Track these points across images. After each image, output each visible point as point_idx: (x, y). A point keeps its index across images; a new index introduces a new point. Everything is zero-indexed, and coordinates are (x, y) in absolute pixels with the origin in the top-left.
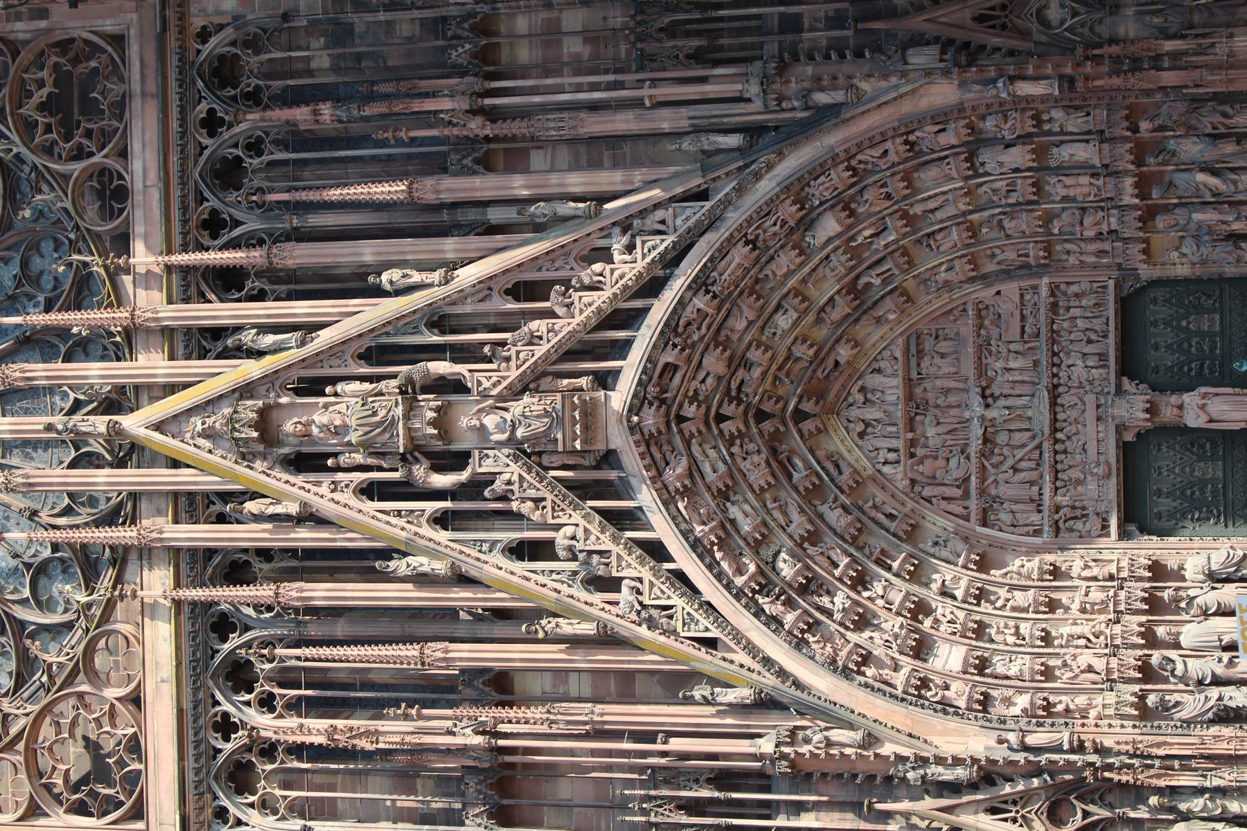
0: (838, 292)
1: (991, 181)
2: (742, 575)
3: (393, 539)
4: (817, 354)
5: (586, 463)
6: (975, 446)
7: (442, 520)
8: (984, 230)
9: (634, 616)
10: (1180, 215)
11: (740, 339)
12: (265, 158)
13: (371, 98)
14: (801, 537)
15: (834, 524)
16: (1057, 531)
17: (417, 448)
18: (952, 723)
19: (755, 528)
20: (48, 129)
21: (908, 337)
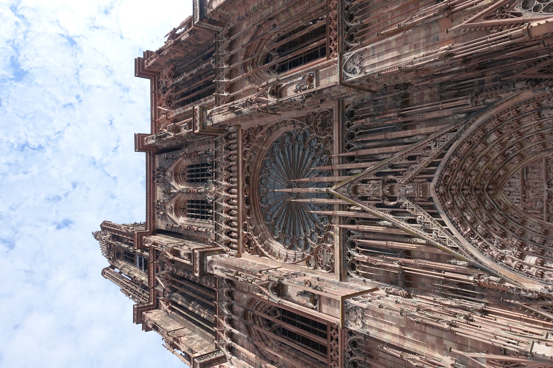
0: (499, 155)
1: (547, 120)
2: (466, 231)
4: (493, 173)
6: (545, 199)
7: (392, 213)
8: (547, 136)
9: (436, 239)
11: (468, 169)
12: (359, 132)
13: (378, 115)
14: (486, 222)
15: (497, 219)
17: (386, 196)
19: (471, 219)
21: (523, 168)
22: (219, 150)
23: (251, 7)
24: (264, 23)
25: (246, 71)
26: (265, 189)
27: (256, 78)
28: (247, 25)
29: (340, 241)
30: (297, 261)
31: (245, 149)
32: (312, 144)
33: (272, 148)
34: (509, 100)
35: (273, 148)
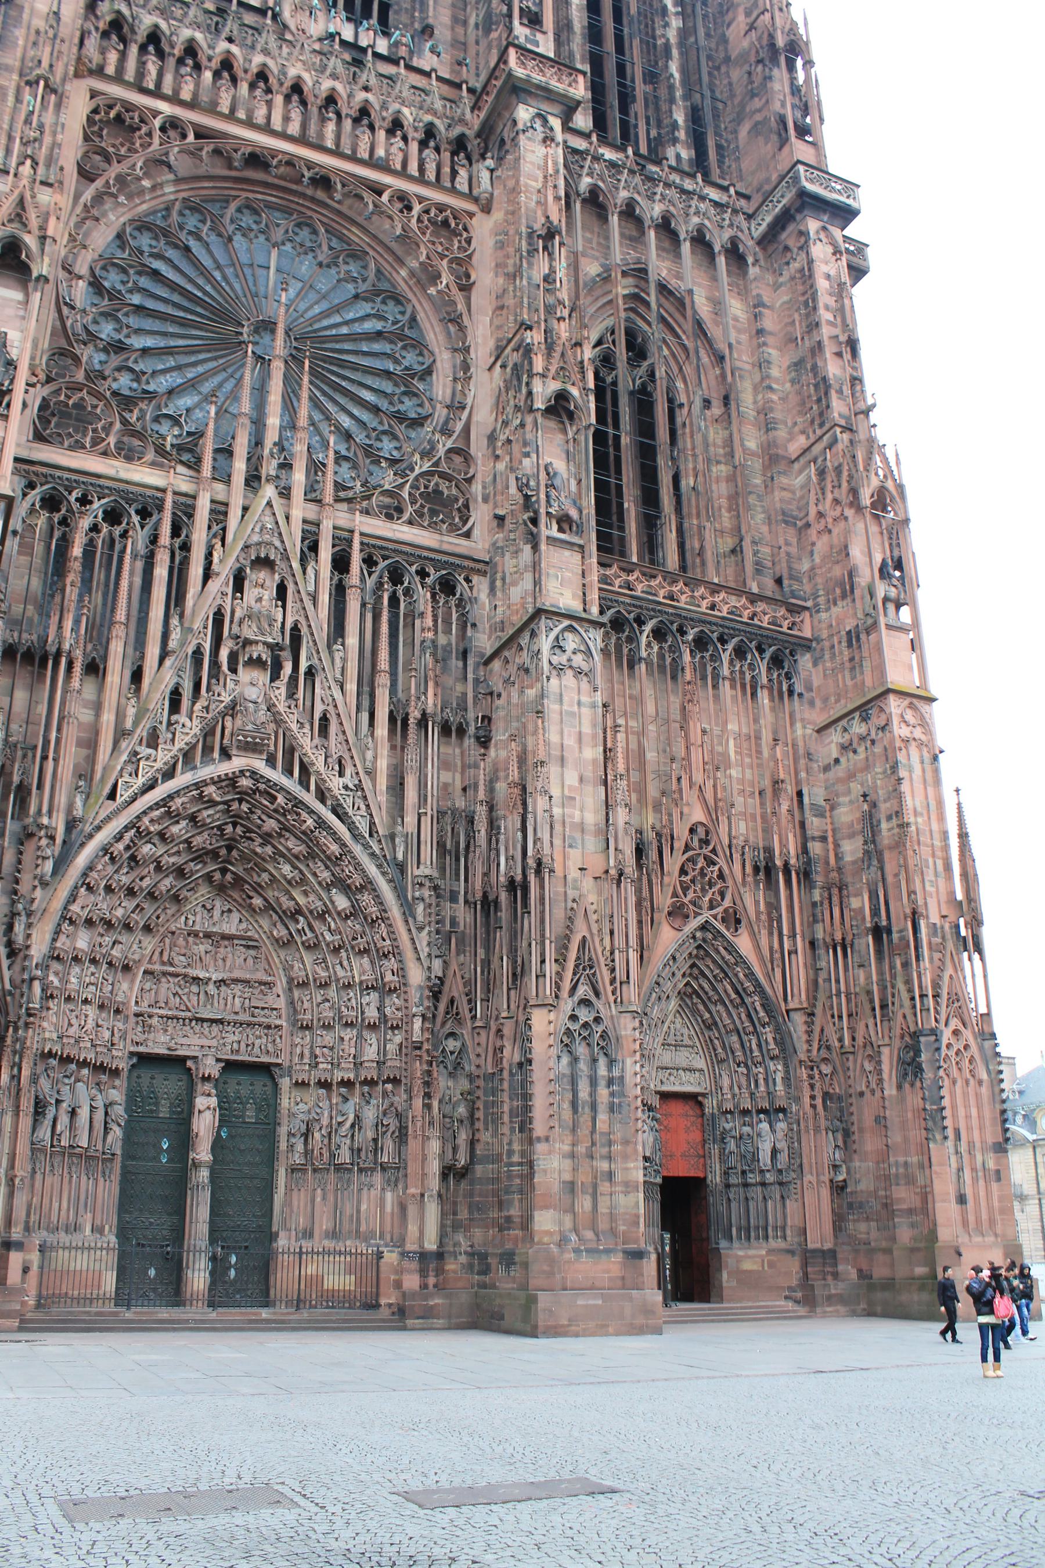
0: (297, 904)
3: (192, 622)
5: (225, 741)
6: (193, 972)
7: (198, 653)
10: (325, 1104)
16: (137, 1015)
17: (244, 646)
18: (48, 937)
20: (426, 487)
22: (428, 99)
23: (774, 352)
24: (723, 376)
25: (624, 274)
26: (278, 235)
27: (597, 299)
28: (736, 319)
29: (127, 482)
30: (65, 310)
31: (417, 208)
32: (385, 438)
33: (397, 299)
34: (414, 943)
35: (398, 302)
